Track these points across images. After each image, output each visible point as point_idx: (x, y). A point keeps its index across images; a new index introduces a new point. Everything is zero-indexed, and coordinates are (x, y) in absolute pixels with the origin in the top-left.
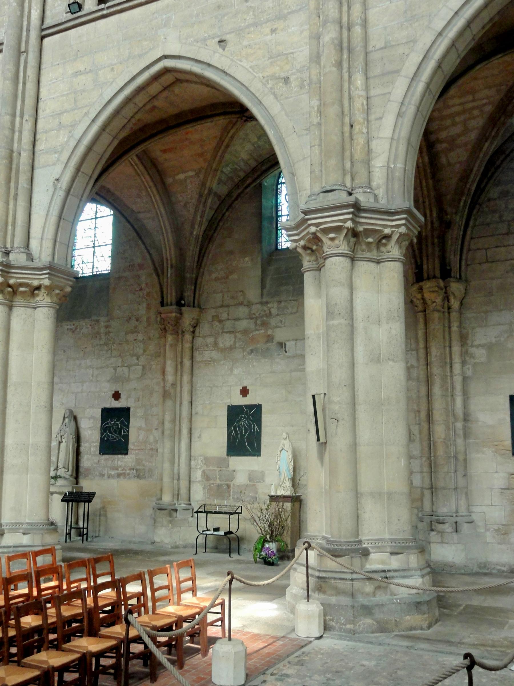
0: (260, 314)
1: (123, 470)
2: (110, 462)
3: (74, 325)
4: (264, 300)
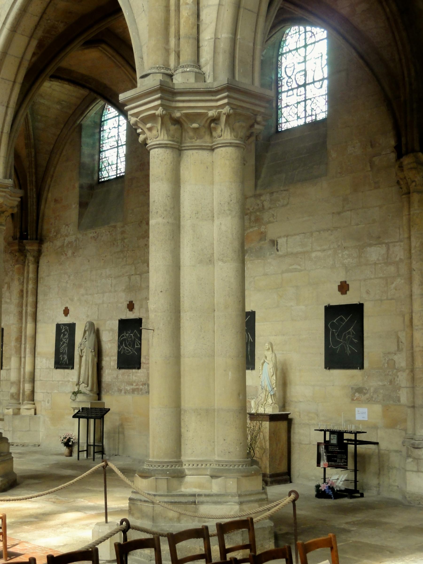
0: (254, 208)
1: (137, 385)
2: (126, 377)
3: (96, 232)
4: (258, 192)
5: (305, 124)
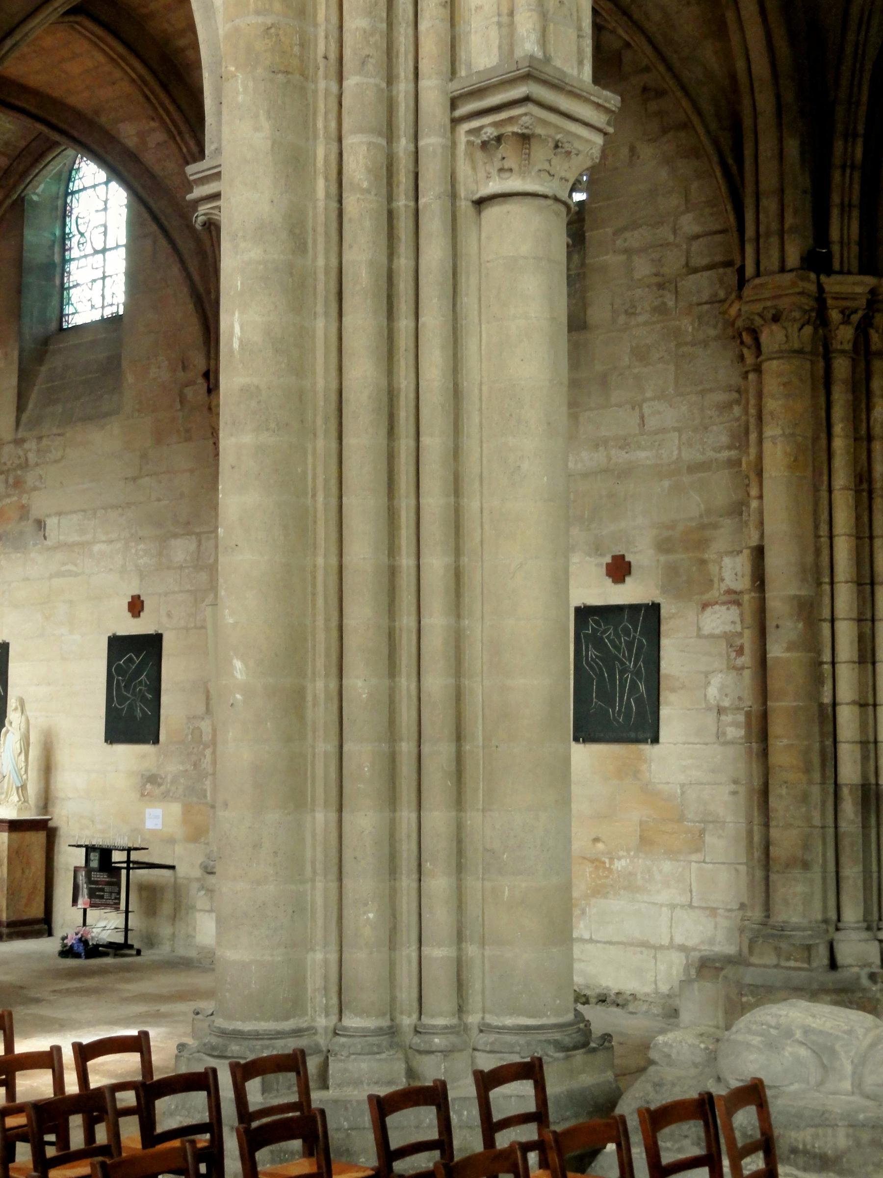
0: (13, 463)
4: (20, 435)
5: (103, 321)
